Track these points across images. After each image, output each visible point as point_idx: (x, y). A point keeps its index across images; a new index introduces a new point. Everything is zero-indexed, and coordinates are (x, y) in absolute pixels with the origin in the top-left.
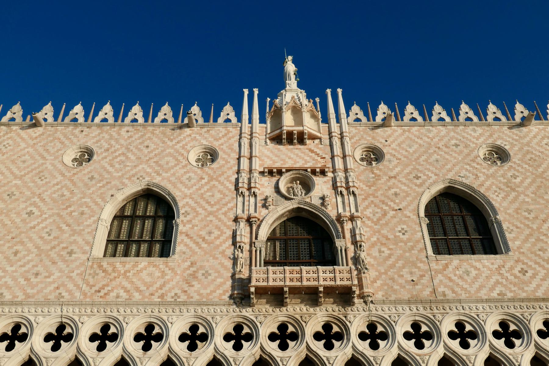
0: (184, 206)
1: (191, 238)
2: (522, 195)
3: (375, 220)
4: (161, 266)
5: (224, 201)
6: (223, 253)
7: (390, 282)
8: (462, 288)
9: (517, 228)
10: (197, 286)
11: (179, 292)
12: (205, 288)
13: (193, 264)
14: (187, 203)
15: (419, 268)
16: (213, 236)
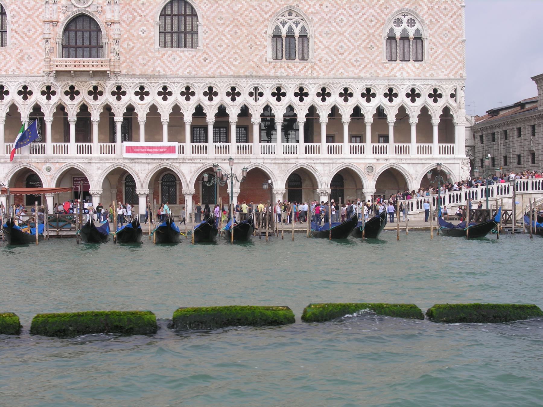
0: (11, 12)
1: (18, 34)
2: (220, 7)
3: (128, 23)
4: (3, 52)
5: (36, 7)
6: (38, 44)
7: (131, 64)
8: (170, 69)
9: (211, 30)
10: (25, 65)
11: (15, 68)
12: (29, 66)
13: (21, 51)
14: (14, 8)
15: (148, 56)
16: (31, 32)
